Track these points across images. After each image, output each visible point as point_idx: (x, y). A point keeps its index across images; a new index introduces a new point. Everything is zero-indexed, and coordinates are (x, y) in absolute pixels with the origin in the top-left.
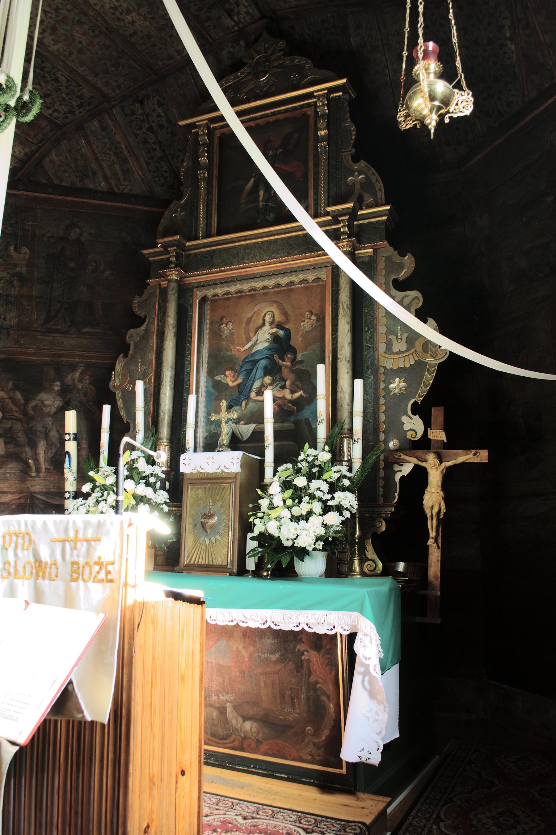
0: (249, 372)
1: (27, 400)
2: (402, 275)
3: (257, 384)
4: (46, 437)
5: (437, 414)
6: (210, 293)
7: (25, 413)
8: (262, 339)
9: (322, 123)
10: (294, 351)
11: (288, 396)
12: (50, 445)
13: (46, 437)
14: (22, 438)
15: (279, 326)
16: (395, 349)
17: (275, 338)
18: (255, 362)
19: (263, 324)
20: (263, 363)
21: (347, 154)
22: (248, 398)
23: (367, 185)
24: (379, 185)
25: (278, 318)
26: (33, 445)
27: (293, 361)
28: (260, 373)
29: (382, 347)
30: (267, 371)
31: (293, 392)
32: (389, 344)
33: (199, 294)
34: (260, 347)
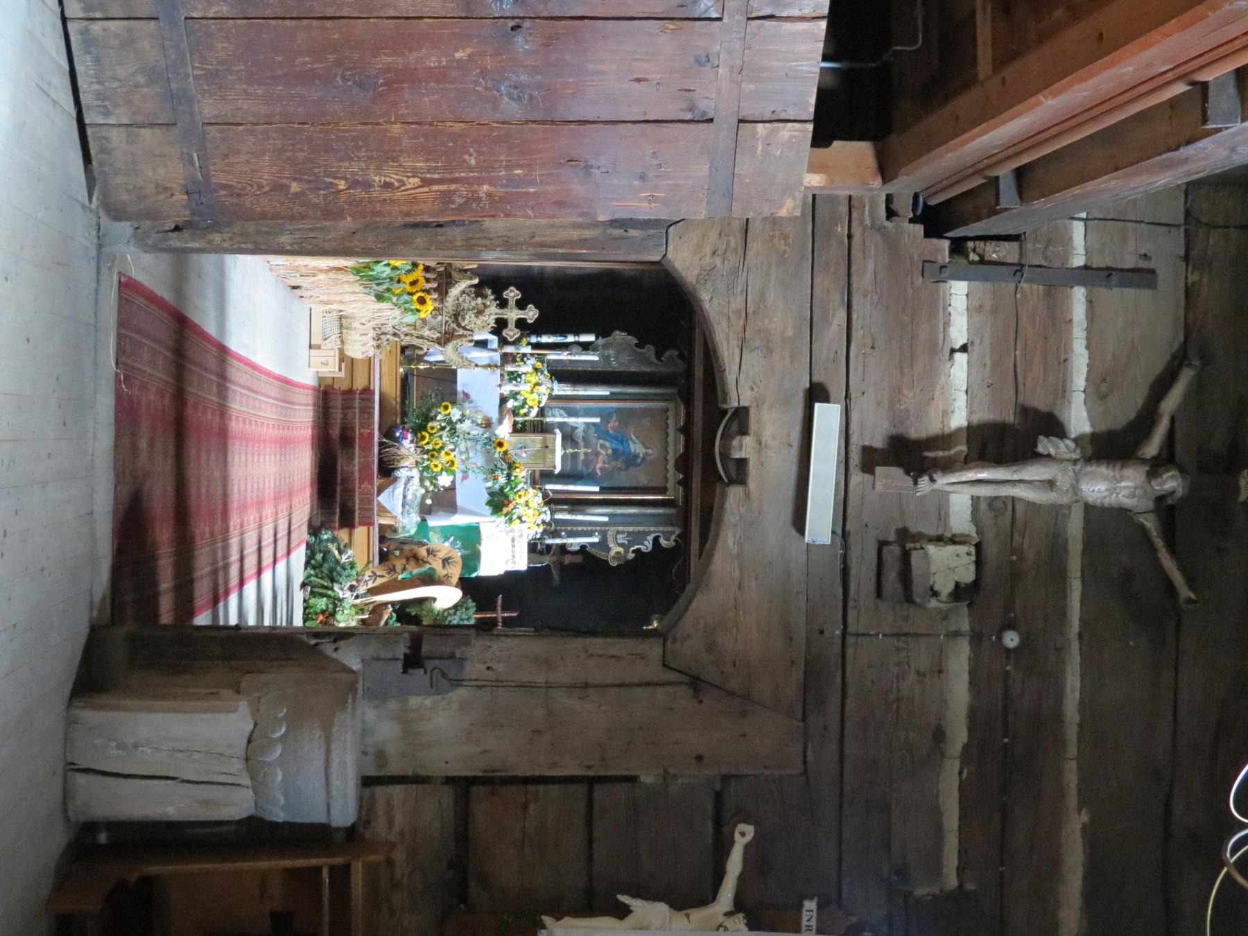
0: (616, 439)
2: (663, 542)
3: (607, 444)
5: (579, 559)
8: (636, 448)
10: (627, 469)
11: (599, 466)
15: (644, 459)
16: (619, 536)
17: (636, 456)
18: (622, 442)
19: (646, 448)
20: (621, 448)
22: (599, 438)
25: (649, 458)
27: (620, 469)
28: (615, 446)
29: (621, 528)
30: (615, 451)
31: (601, 469)
32: (623, 532)
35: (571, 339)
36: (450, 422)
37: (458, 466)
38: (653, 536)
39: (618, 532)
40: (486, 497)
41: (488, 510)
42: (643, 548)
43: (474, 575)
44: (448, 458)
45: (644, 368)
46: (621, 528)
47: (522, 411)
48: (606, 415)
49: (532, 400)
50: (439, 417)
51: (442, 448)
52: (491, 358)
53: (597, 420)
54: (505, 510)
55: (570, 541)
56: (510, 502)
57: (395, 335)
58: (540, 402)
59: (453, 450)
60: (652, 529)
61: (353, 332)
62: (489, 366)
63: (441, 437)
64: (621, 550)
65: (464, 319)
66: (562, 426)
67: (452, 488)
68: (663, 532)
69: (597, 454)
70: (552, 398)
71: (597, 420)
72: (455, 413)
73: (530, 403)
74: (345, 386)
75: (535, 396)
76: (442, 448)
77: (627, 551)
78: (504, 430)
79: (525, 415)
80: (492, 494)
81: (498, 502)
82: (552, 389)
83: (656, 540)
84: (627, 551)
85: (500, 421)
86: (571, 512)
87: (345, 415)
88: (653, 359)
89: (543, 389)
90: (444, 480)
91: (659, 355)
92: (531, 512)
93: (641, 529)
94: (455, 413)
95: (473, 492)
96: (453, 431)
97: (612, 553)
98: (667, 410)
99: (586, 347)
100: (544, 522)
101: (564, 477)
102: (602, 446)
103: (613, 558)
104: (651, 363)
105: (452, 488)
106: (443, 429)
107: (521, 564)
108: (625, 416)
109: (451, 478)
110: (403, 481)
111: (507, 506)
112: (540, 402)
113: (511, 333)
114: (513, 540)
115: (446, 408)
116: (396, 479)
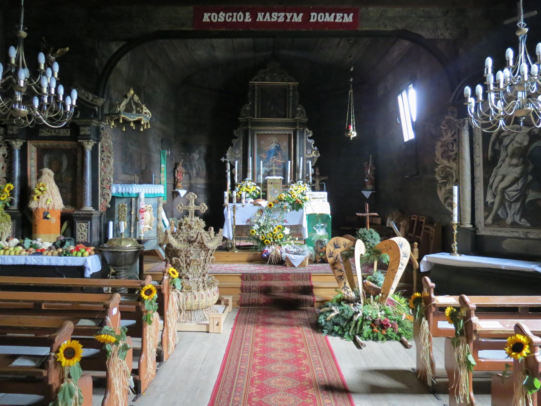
0: (269, 155)
1: (190, 155)
2: (310, 135)
4: (195, 167)
5: (317, 169)
6: (259, 133)
7: (189, 160)
8: (273, 147)
9: (291, 93)
10: (281, 150)
12: (196, 169)
13: (195, 167)
14: (189, 167)
15: (277, 143)
17: (276, 146)
20: (273, 153)
21: (297, 102)
22: (269, 161)
23: (301, 111)
24: (305, 112)
26: (192, 170)
28: (272, 155)
29: (305, 152)
30: (274, 155)
32: (307, 151)
33: (256, 132)
34: (272, 148)
35: (229, 174)
36: (259, 230)
37: (280, 225)
38: (308, 139)
39: (307, 153)
40: (295, 211)
41: (300, 211)
42: (313, 143)
43: (330, 217)
44: (277, 230)
45: (241, 144)
46: (305, 152)
47: (258, 192)
48: (260, 158)
49: (253, 189)
50: (258, 234)
51: (272, 233)
52: (231, 210)
53: (262, 162)
54: (301, 203)
55: (310, 172)
56: (297, 201)
57: (204, 275)
58: (254, 185)
59: (273, 228)
60: (305, 140)
61: (201, 303)
62: (234, 211)
63: (267, 234)
64: (313, 152)
65: (193, 237)
66: (264, 176)
67: (291, 227)
68: (306, 135)
69: (276, 162)
70: (253, 180)
71: (262, 162)
72: (256, 227)
73: (255, 189)
74: (239, 291)
75: (251, 188)
76: (272, 233)
77: (314, 150)
78: (264, 203)
79: (259, 191)
80: (293, 209)
81: (297, 206)
82: (249, 180)
83: (310, 138)
84: (314, 150)
85: (260, 205)
86: (299, 172)
87: (254, 291)
88: (237, 140)
89: (249, 184)
90: (287, 231)
91: (236, 138)
92: (299, 189)
93: (305, 144)
94: (256, 227)
95: (292, 217)
96: (264, 227)
97: (315, 156)
98: (258, 134)
99: (232, 167)
100: (303, 183)
101: (285, 175)
102: (272, 160)
103: (317, 155)
104: (239, 141)
105: (291, 227)
106: (263, 233)
107: (325, 194)
108: (260, 151)
109: (286, 228)
110: (287, 254)
111: (298, 202)
112: (254, 185)
113: (203, 208)
114: (314, 198)
115: (253, 232)
116: (287, 258)
